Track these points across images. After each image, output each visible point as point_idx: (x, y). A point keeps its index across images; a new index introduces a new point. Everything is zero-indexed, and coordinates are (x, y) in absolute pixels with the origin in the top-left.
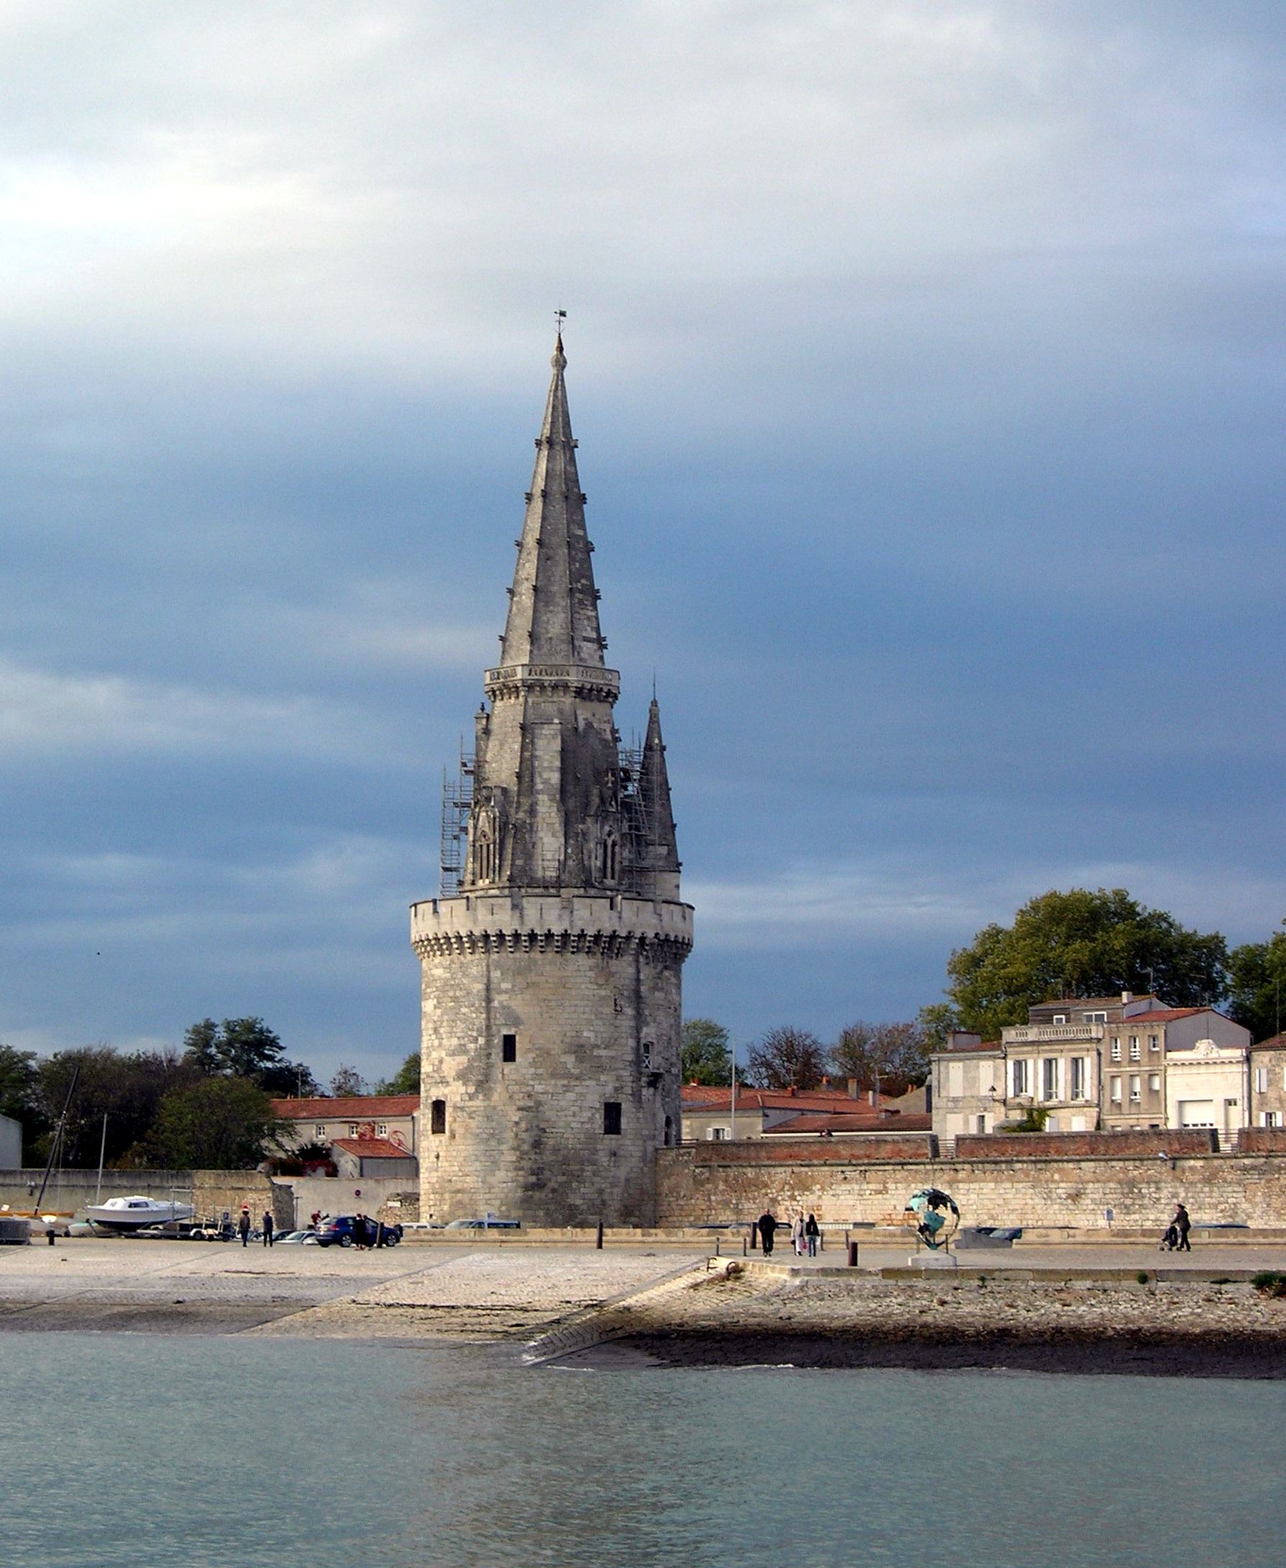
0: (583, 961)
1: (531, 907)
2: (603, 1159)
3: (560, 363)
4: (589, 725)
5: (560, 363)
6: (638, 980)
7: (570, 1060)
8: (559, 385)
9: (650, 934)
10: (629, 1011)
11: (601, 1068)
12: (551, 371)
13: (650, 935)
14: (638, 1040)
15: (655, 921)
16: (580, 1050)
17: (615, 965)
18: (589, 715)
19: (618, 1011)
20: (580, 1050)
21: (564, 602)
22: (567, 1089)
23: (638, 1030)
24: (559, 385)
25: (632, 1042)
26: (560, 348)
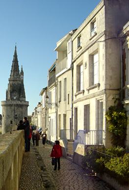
0: (9, 107)
3: (16, 48)
5: (16, 48)
8: (16, 50)
10: (13, 112)
24: (16, 50)
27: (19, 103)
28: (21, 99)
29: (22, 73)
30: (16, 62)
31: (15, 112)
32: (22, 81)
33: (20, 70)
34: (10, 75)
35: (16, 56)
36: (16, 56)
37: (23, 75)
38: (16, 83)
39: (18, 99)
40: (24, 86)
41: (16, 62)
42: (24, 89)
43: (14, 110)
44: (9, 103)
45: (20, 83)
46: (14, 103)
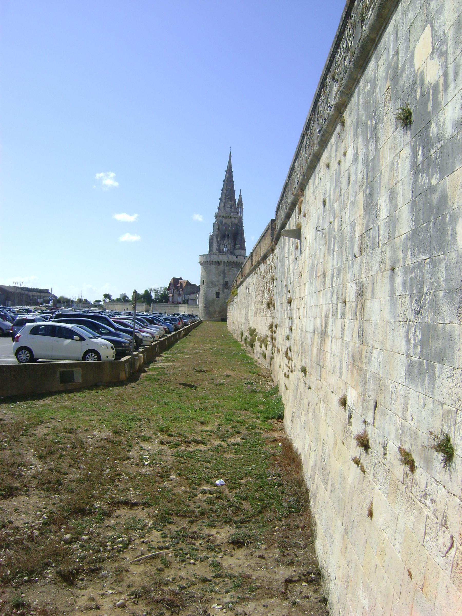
0: (213, 266)
1: (221, 257)
2: (216, 302)
3: (230, 156)
4: (225, 223)
5: (230, 156)
6: (224, 270)
7: (211, 284)
8: (230, 161)
9: (226, 261)
10: (222, 275)
11: (216, 286)
12: (229, 158)
13: (226, 261)
14: (224, 281)
15: (227, 258)
16: (212, 283)
17: (219, 267)
18: (226, 221)
19: (219, 275)
20: (212, 283)
21: (224, 201)
22: (210, 290)
23: (224, 278)
24: (230, 161)
25: (222, 281)
26: (230, 154)
27: (233, 258)
28: (237, 252)
29: (240, 201)
30: (229, 182)
31: (224, 277)
32: (240, 219)
33: (237, 197)
34: (219, 208)
35: (229, 172)
36: (229, 172)
37: (242, 208)
38: (228, 222)
39: (232, 253)
40: (244, 229)
41: (229, 182)
42: (242, 234)
43: (224, 272)
44: (215, 258)
45: (236, 221)
46: (224, 258)
